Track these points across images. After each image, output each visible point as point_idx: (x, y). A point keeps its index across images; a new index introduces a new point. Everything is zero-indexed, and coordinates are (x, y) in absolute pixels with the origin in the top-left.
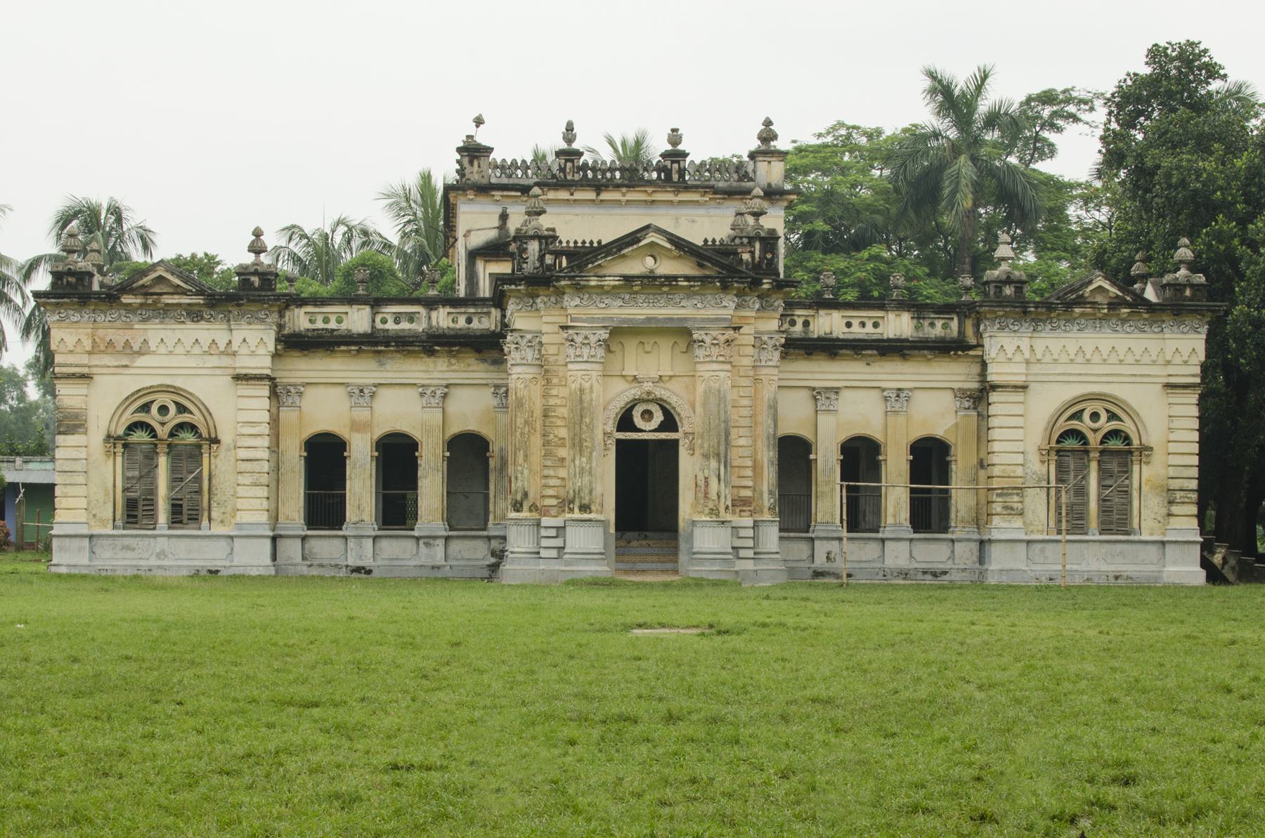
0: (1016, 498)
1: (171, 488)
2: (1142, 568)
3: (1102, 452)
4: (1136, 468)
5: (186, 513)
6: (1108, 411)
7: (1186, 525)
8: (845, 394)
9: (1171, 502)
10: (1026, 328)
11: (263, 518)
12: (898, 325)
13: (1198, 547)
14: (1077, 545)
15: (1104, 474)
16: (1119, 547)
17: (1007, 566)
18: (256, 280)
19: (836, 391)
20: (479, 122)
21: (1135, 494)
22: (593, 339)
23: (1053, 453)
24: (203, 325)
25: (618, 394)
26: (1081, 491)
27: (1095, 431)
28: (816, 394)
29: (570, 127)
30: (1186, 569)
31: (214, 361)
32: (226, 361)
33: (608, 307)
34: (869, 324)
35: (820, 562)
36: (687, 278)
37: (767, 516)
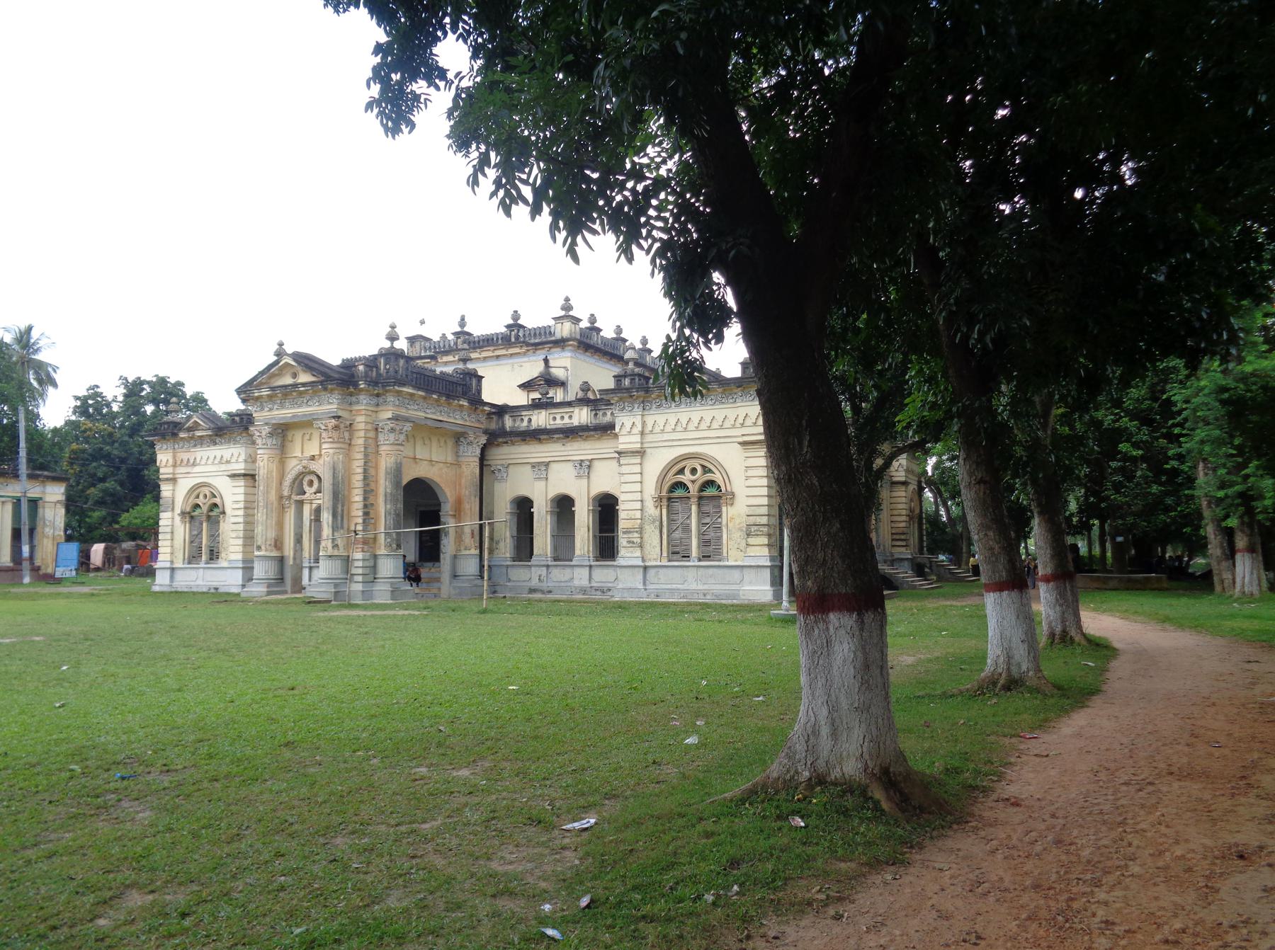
0: (636, 535)
1: (208, 540)
2: (727, 587)
3: (700, 498)
4: (724, 509)
5: (214, 555)
6: (703, 466)
7: (760, 553)
8: (553, 466)
9: (748, 535)
10: (638, 411)
11: (240, 557)
12: (581, 416)
13: (768, 571)
14: (680, 570)
15: (701, 513)
16: (711, 571)
17: (629, 585)
18: (237, 419)
19: (547, 464)
20: (422, 322)
21: (724, 529)
22: (264, 433)
23: (665, 503)
24: (217, 447)
25: (293, 467)
26: (687, 529)
27: (693, 482)
28: (533, 466)
29: (463, 319)
30: (759, 589)
31: (223, 467)
32: (230, 467)
33: (271, 410)
34: (566, 417)
35: (535, 583)
36: (304, 385)
37: (382, 551)
